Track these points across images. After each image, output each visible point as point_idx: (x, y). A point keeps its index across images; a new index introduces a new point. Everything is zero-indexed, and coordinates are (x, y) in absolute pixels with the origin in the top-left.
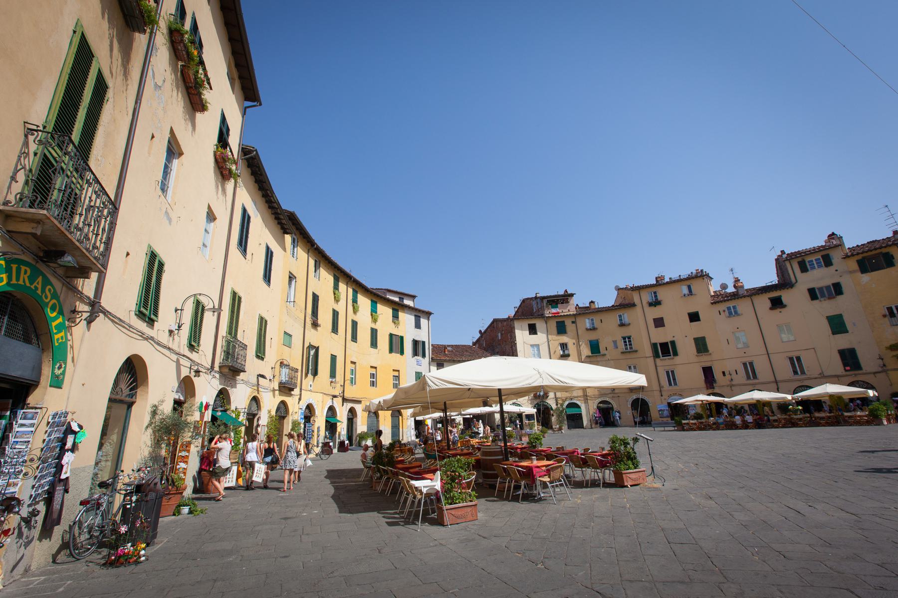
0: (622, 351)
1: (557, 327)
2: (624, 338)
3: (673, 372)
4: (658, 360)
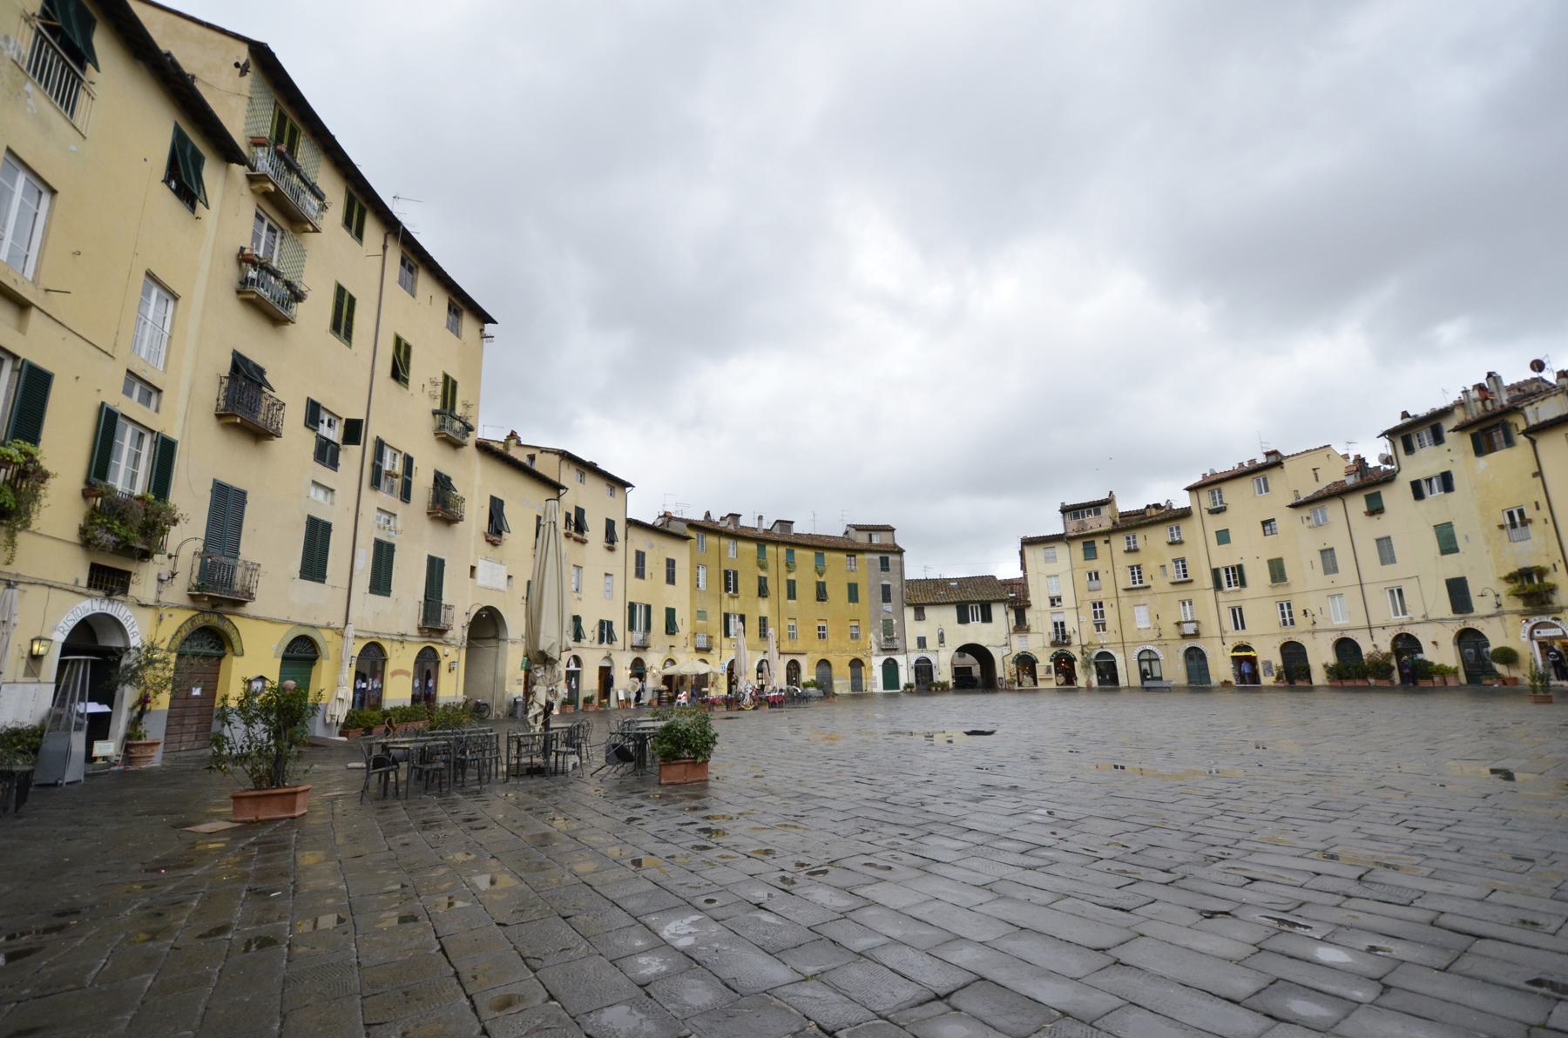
1: (1084, 549)
2: (1176, 561)
3: (1240, 609)
4: (1220, 594)
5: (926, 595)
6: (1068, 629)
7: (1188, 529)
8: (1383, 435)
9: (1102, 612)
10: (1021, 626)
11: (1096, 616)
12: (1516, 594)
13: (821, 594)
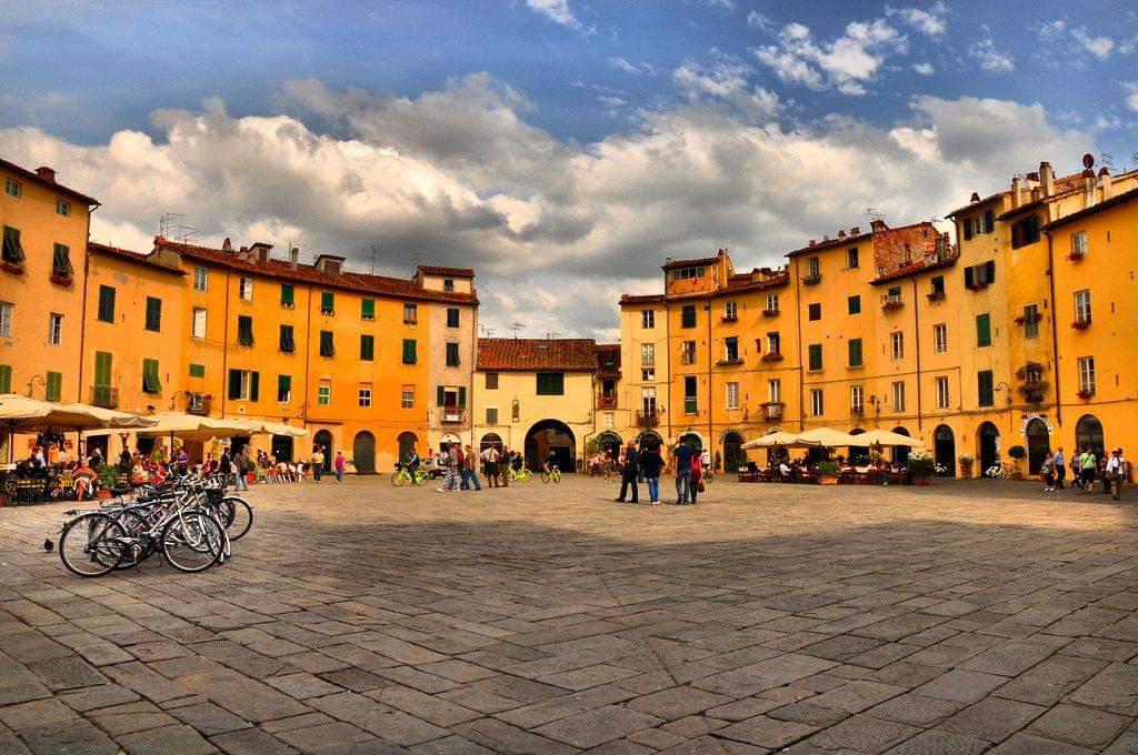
1: (683, 315)
2: (770, 335)
3: (821, 393)
5: (499, 358)
6: (658, 407)
7: (786, 300)
8: (949, 217)
10: (607, 400)
12: (1022, 390)
13: (367, 348)
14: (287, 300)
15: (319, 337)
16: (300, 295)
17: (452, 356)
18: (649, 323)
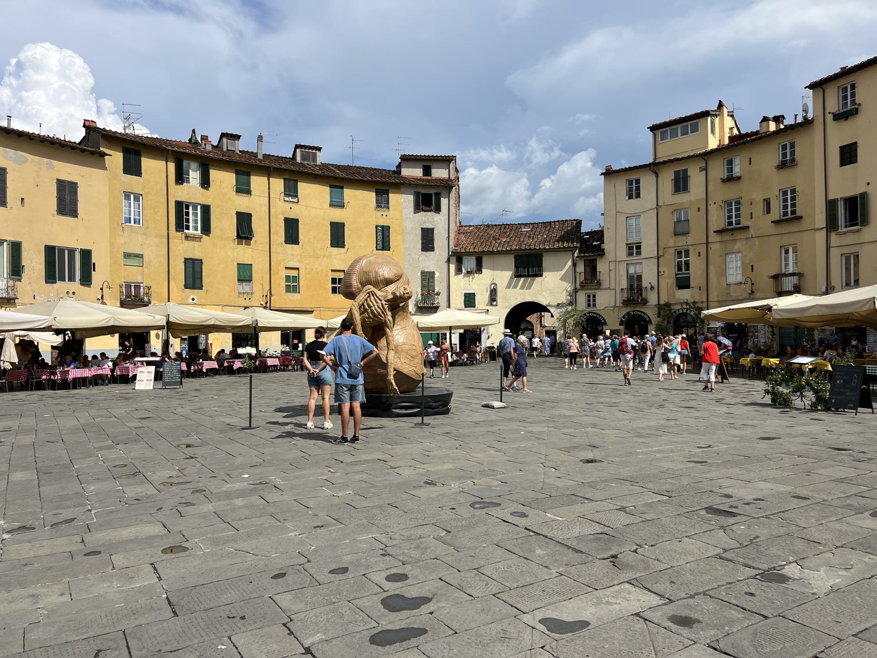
0: (777, 218)
3: (857, 257)
4: (833, 236)
6: (645, 284)
9: (687, 264)
11: (680, 269)
14: (243, 189)
15: (282, 224)
16: (258, 182)
17: (427, 240)
18: (634, 192)
